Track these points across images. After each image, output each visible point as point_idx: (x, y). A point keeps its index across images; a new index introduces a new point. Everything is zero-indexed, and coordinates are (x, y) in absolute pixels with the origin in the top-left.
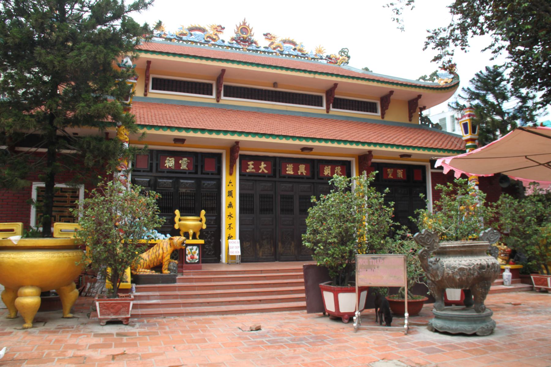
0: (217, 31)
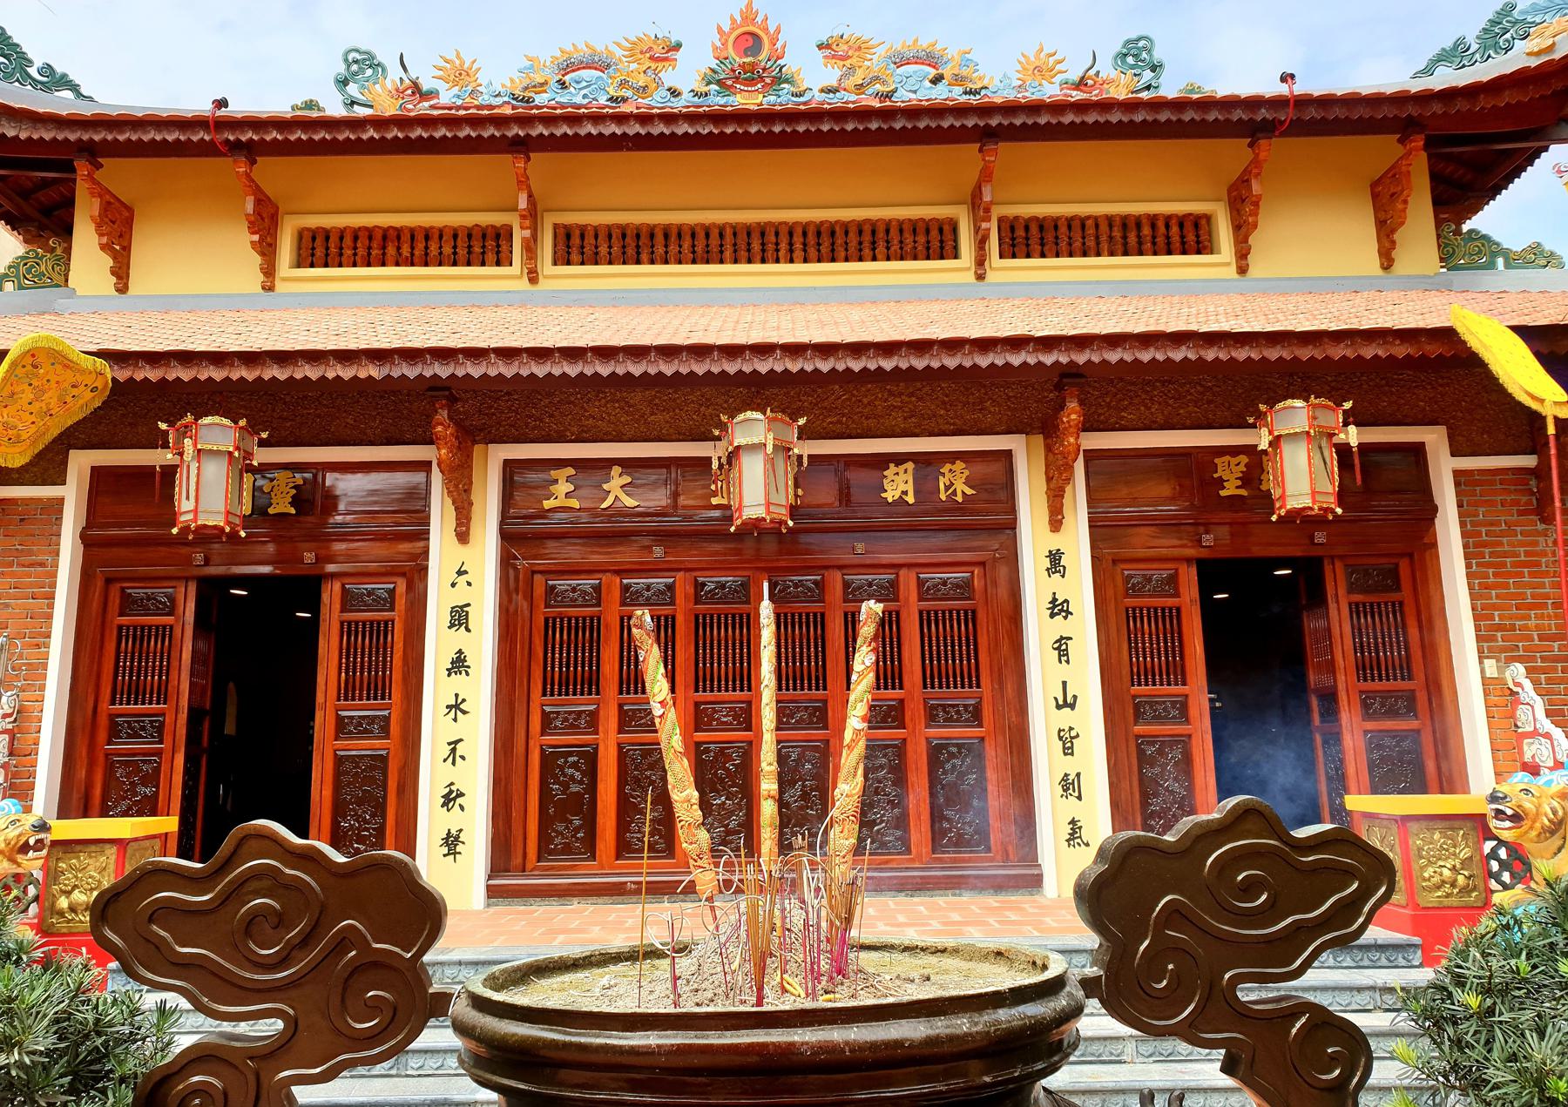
0: (652, 58)
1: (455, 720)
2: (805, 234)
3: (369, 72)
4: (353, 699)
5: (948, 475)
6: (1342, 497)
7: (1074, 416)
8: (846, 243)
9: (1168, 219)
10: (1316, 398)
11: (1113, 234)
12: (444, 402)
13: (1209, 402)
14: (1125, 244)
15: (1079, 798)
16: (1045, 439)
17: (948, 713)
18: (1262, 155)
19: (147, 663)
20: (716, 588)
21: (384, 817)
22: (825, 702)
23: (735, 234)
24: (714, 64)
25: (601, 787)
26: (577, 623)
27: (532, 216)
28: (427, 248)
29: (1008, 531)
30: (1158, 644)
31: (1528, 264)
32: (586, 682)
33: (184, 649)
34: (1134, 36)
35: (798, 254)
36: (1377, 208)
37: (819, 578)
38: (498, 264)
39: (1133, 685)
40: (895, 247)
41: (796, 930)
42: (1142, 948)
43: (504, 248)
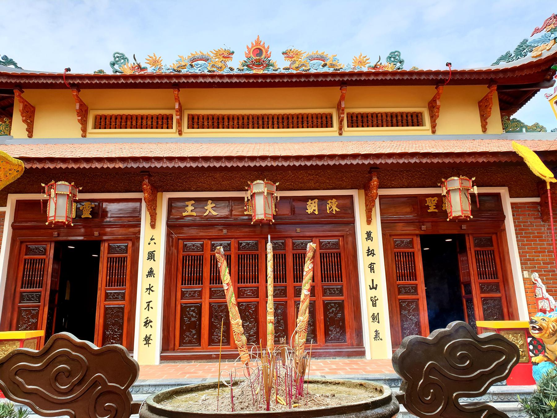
0: (223, 57)
1: (149, 294)
2: (278, 118)
3: (122, 61)
4: (112, 286)
5: (330, 204)
6: (472, 212)
7: (375, 183)
8: (293, 122)
9: (407, 114)
10: (462, 176)
11: (388, 119)
12: (147, 176)
13: (423, 178)
14: (392, 123)
15: (378, 322)
16: (365, 191)
17: (330, 291)
18: (440, 91)
19: (35, 273)
20: (246, 245)
21: (122, 330)
22: (286, 287)
23: (253, 118)
24: (245, 59)
25: (203, 319)
26: (195, 258)
27: (180, 111)
28: (142, 122)
29: (352, 224)
30: (406, 265)
31: (534, 130)
32: (198, 280)
33: (49, 267)
34: (394, 51)
35: (276, 125)
36: (480, 111)
37: (283, 241)
38: (168, 128)
39: (398, 281)
40: (310, 123)
41: (281, 377)
42: (420, 383)
43: (170, 122)
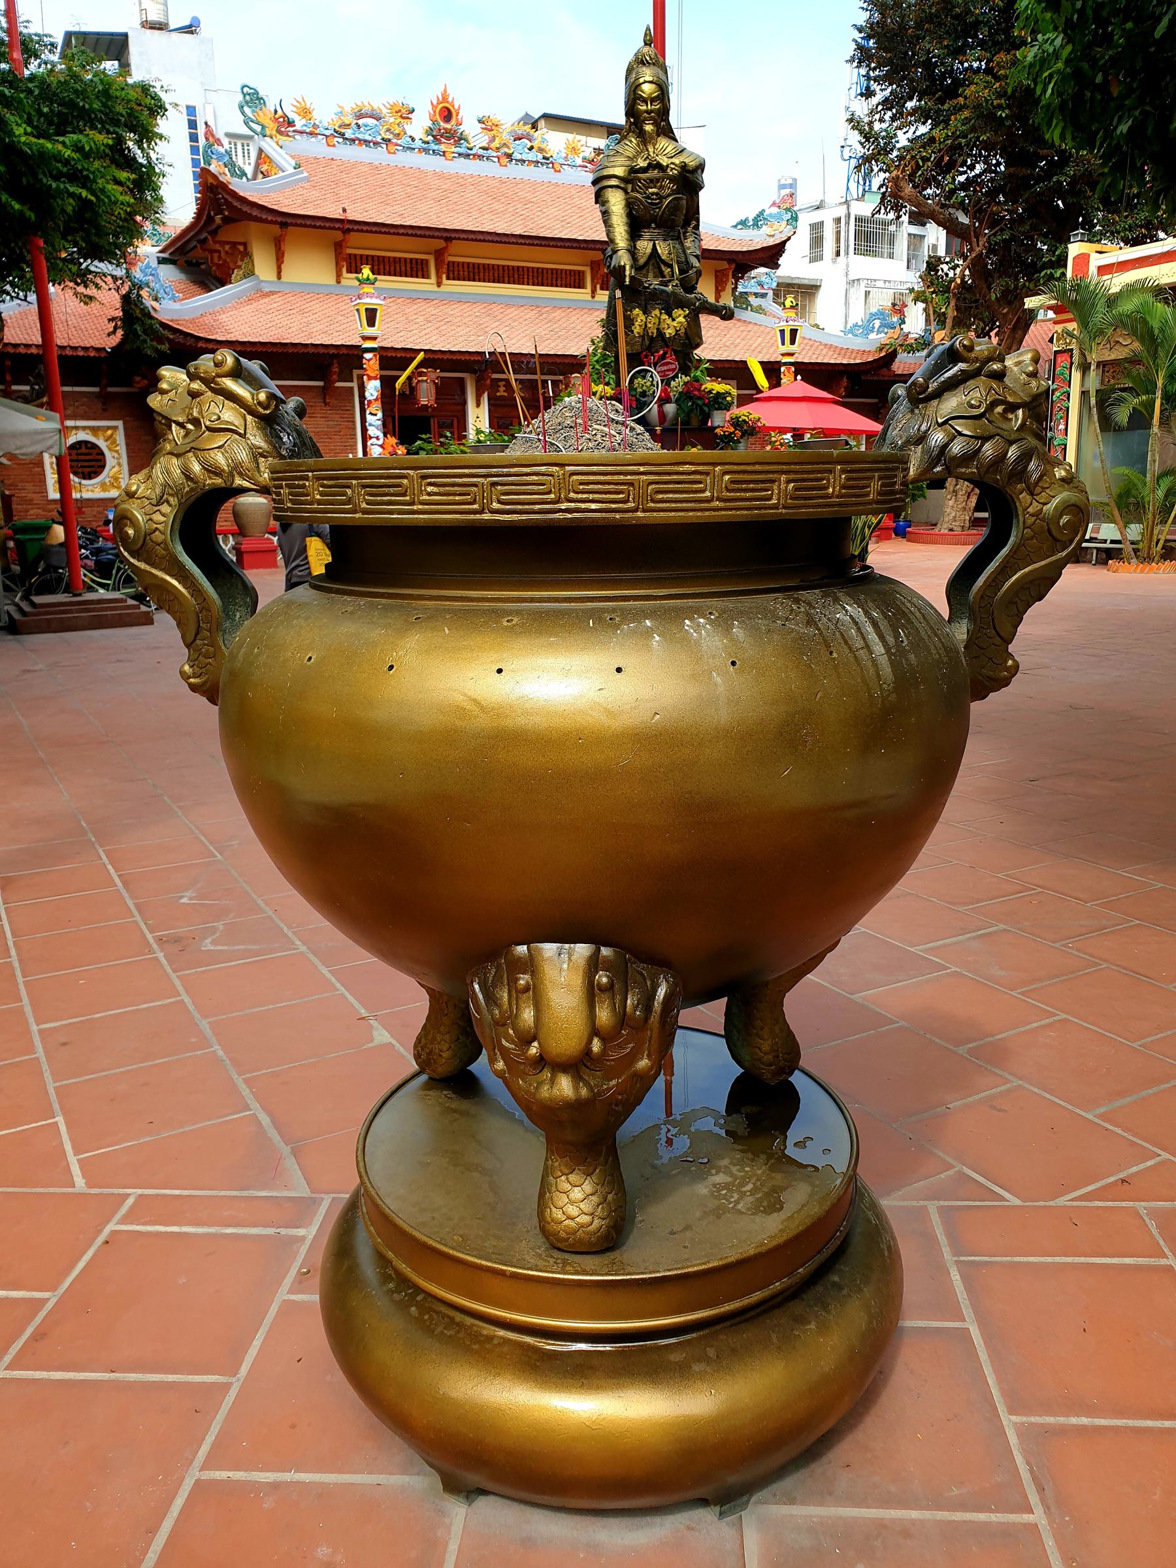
0: (401, 116)
36: (716, 282)
38: (423, 277)
43: (425, 269)
